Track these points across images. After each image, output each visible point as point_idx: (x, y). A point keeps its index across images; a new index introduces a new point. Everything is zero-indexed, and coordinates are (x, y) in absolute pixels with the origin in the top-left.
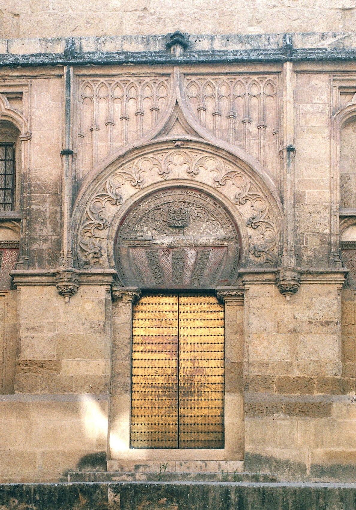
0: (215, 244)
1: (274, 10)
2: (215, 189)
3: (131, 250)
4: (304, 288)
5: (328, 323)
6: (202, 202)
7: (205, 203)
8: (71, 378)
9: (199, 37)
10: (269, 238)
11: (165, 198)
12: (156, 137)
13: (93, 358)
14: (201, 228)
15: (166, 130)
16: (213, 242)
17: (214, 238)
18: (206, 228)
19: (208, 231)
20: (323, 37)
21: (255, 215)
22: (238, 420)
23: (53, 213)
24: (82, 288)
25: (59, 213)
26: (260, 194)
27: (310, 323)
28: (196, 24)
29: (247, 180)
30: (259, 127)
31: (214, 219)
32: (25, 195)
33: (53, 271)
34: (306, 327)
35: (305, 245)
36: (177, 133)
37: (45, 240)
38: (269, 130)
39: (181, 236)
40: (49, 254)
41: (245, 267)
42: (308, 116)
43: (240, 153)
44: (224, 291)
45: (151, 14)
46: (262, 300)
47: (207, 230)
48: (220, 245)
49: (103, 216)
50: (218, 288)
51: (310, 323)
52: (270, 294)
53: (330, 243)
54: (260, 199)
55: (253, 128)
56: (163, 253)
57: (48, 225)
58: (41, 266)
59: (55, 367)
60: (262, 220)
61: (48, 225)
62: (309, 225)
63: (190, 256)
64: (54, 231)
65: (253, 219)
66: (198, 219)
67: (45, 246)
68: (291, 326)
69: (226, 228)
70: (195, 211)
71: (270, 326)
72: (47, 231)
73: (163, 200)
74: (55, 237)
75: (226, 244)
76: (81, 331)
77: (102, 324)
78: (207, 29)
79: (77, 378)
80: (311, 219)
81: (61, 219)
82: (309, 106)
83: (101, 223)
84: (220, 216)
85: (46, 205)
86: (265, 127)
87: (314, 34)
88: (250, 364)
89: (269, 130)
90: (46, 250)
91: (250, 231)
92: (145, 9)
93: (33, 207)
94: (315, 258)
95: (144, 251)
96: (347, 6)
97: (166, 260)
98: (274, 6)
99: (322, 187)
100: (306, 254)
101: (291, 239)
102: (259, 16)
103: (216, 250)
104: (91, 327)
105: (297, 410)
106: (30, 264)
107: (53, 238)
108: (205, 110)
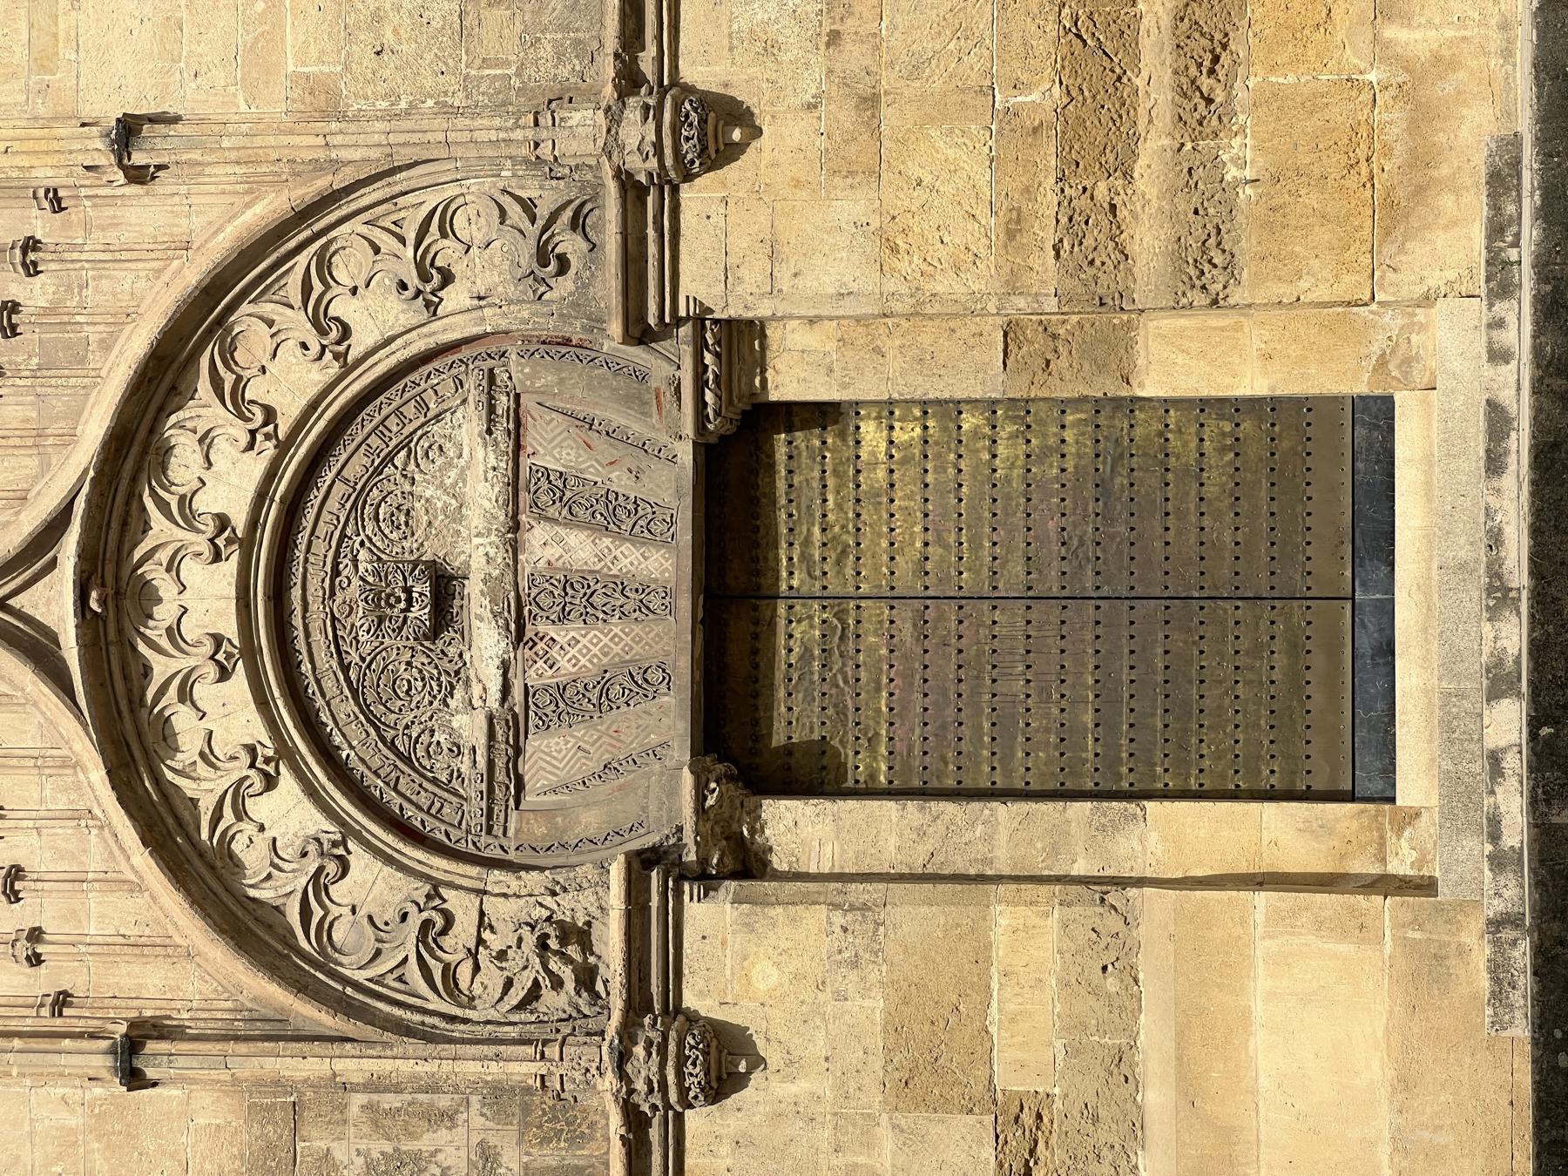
0: (505, 444)
2: (284, 447)
3: (529, 799)
4: (695, 72)
6: (333, 504)
7: (340, 489)
8: (1071, 1052)
10: (482, 220)
11: (317, 660)
13: (982, 957)
14: (439, 505)
16: (499, 455)
17: (480, 453)
18: (441, 485)
19: (453, 474)
21: (387, 282)
22: (1255, 335)
23: (376, 1124)
24: (690, 1000)
25: (375, 1097)
26: (302, 260)
27: (834, 38)
29: (248, 323)
30: (32, 270)
31: (403, 453)
33: (616, 1123)
34: (853, 55)
35: (511, 71)
38: (40, 224)
39: (474, 588)
40: (545, 1141)
41: (596, 323)
43: (137, 344)
44: (700, 404)
46: (740, 243)
47: (448, 482)
48: (511, 426)
49: (391, 914)
50: (688, 429)
51: (834, 38)
52: (716, 209)
54: (324, 263)
56: (540, 663)
57: (425, 1143)
59: (1028, 1119)
60: (410, 252)
61: (425, 1143)
62: (429, 57)
63: (553, 552)
64: (447, 1118)
65: (403, 286)
66: (402, 519)
68: (846, 116)
69: (441, 400)
70: (368, 532)
71: (851, 206)
73: (325, 660)
74: (476, 1118)
75: (504, 399)
76: (870, 1008)
77: (838, 919)
79: (1074, 1026)
80: (404, 47)
81: (397, 1089)
83: (415, 920)
84: (395, 429)
85: (340, 1153)
86: (31, 244)
88: (1012, 286)
89: (40, 224)
90: (528, 1154)
91: (454, 298)
94: (565, 28)
97: (573, 652)
100: (548, 68)
101: (488, 128)
103: (531, 440)
104: (855, 964)
105: (1205, 83)
107: (478, 1121)
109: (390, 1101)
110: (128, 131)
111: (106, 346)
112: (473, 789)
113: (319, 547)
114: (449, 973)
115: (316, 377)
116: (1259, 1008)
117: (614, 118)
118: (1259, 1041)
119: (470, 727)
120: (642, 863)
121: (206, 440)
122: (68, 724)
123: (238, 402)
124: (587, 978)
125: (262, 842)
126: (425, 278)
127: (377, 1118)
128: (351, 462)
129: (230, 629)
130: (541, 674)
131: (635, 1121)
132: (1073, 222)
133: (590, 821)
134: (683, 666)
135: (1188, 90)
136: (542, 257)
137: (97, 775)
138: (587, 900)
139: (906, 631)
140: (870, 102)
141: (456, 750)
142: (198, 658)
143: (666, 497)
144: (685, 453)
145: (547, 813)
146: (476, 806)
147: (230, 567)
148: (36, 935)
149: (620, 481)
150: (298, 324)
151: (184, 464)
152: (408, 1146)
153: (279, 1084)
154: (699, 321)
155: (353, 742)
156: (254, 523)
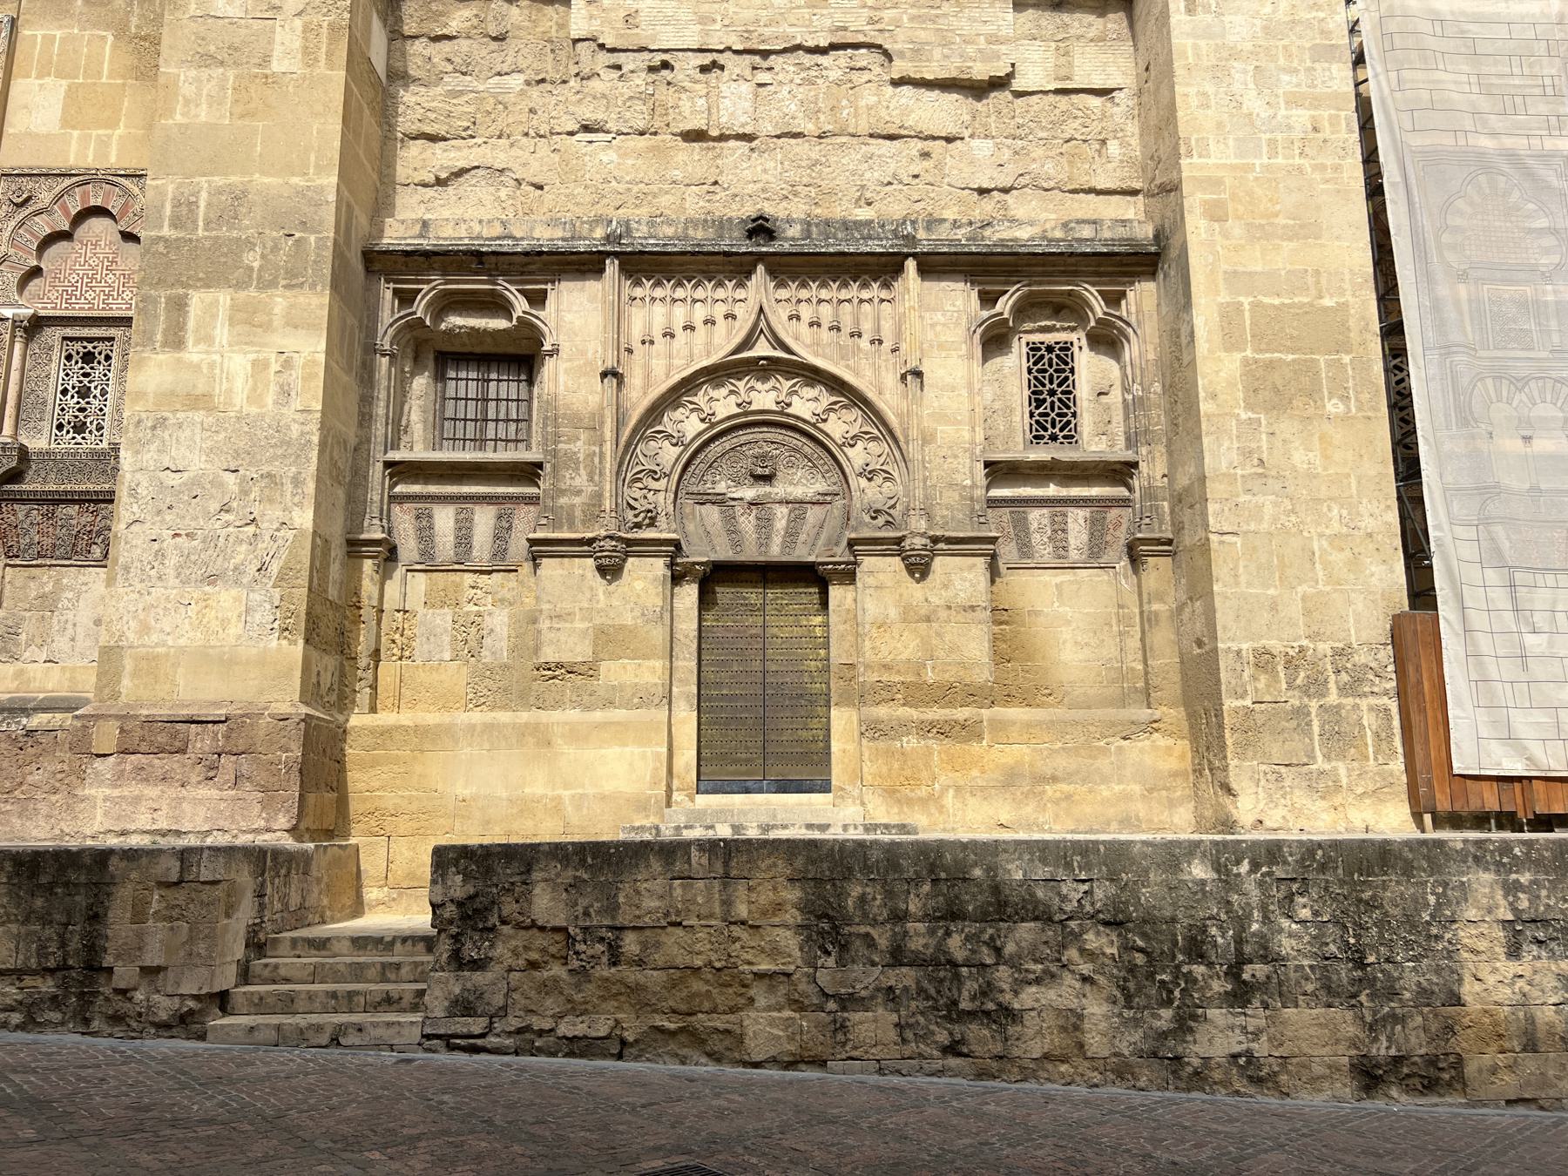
0: (814, 500)
1: (889, 188)
2: (814, 425)
3: (698, 507)
4: (938, 562)
5: (973, 608)
6: (795, 442)
7: (800, 444)
8: (614, 687)
9: (790, 221)
11: (743, 436)
12: (733, 353)
13: (646, 657)
15: (747, 343)
20: (956, 224)
22: (851, 747)
23: (589, 455)
24: (630, 560)
26: (876, 431)
27: (949, 608)
28: (784, 204)
29: (855, 413)
30: (872, 342)
32: (549, 429)
33: (589, 535)
34: (943, 614)
36: (762, 349)
37: (579, 493)
38: (887, 345)
39: (768, 489)
40: (583, 511)
41: (855, 529)
42: (938, 328)
43: (848, 377)
44: (828, 564)
45: (725, 189)
46: (881, 576)
49: (659, 461)
50: (819, 560)
51: (949, 608)
52: (892, 568)
53: (972, 499)
54: (875, 439)
55: (864, 343)
57: (582, 472)
58: (571, 528)
59: (591, 672)
61: (582, 472)
63: (779, 515)
64: (591, 479)
67: (577, 500)
68: (923, 612)
71: (893, 613)
72: (581, 480)
73: (743, 439)
74: (591, 488)
76: (628, 619)
77: (658, 609)
78: (798, 209)
79: (622, 687)
81: (600, 462)
82: (939, 314)
83: (657, 469)
85: (579, 443)
86: (881, 342)
87: (945, 220)
88: (867, 666)
89: (887, 345)
91: (863, 482)
92: (716, 183)
93: (561, 446)
94: (952, 519)
95: (716, 508)
96: (985, 186)
98: (890, 183)
99: (959, 423)
100: (940, 513)
101: (919, 493)
102: (868, 195)
103: (816, 507)
104: (643, 614)
105: (935, 730)
106: (556, 525)
107: (590, 489)
108: (798, 318)
109: (597, 460)
110: (918, 374)
111: (847, 366)
112: (701, 488)
113: (781, 437)
114: (640, 480)
115: (837, 436)
116: (628, 749)
117: (923, 535)
118: (617, 749)
119: (721, 487)
120: (677, 544)
121: (816, 399)
122: (722, 353)
123: (829, 410)
124: (638, 526)
125: (682, 417)
126: (870, 472)
127: (591, 455)
128: (808, 448)
129: (753, 407)
130: (739, 510)
131: (590, 542)
132: (888, 687)
133: (691, 527)
134: (742, 558)
135: (932, 724)
136: (876, 511)
137: (705, 363)
138: (664, 526)
139: (753, 631)
140: (928, 620)
141: (714, 483)
142: (744, 397)
143: (797, 552)
144: (812, 559)
145: (693, 513)
146: (695, 489)
147: (774, 408)
148: (652, 342)
149: (802, 537)
150: (855, 430)
151: (808, 392)
152: (582, 466)
153: (602, 423)
154: (855, 563)
155: (716, 448)
156: (788, 415)
